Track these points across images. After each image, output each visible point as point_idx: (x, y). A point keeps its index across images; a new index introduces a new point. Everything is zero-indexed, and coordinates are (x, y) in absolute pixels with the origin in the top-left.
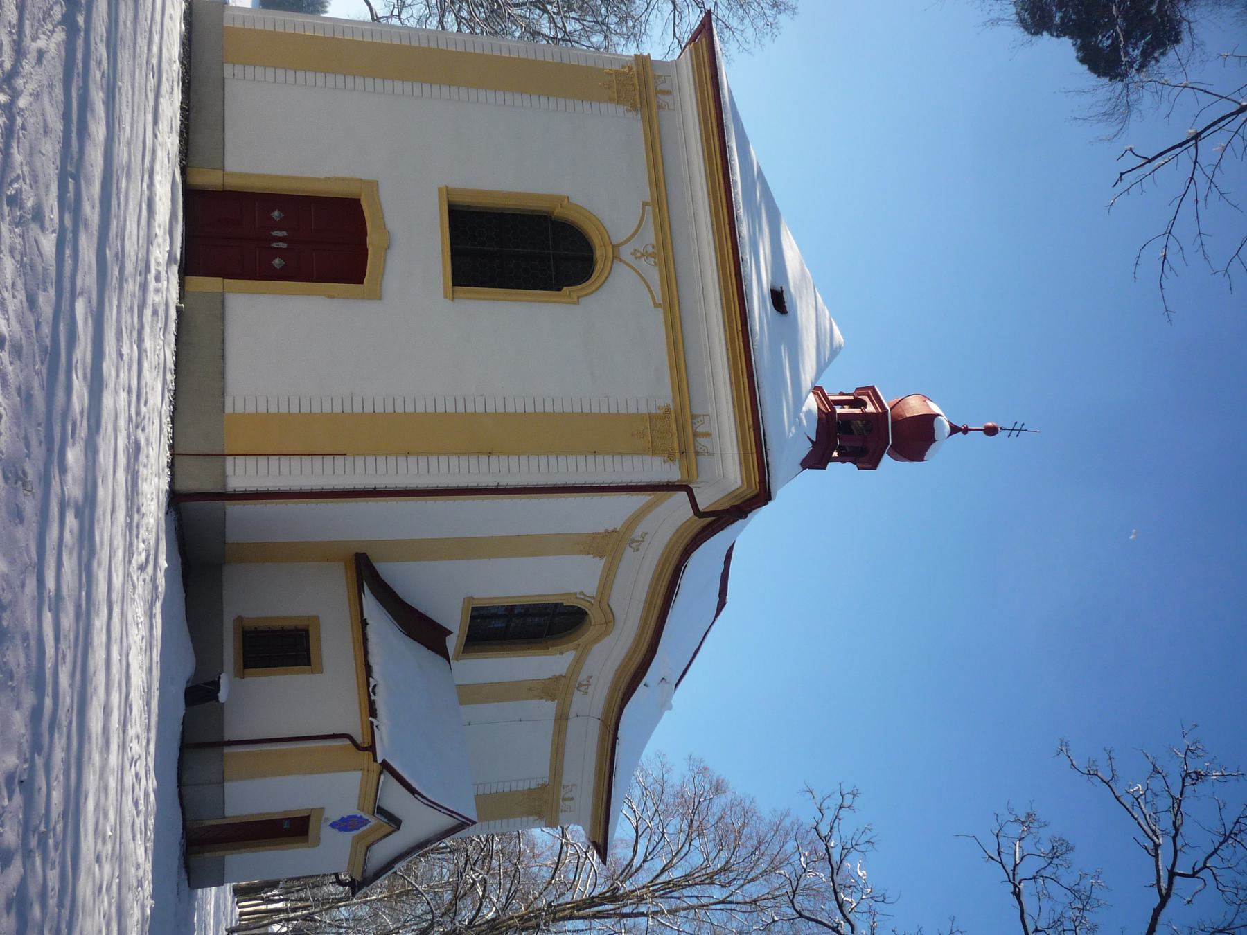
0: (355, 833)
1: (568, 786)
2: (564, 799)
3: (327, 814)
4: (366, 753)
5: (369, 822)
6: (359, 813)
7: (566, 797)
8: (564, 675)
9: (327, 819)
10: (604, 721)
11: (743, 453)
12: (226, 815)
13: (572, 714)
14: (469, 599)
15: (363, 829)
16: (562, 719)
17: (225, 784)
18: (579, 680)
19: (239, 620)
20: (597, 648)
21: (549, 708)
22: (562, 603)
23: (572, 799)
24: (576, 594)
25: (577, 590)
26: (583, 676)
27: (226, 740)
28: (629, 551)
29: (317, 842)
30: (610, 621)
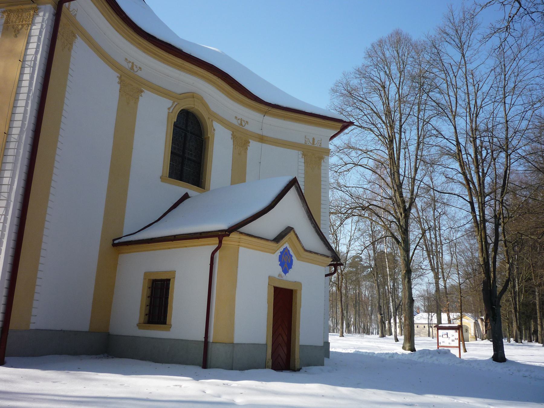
0: (294, 258)
1: (305, 141)
2: (313, 144)
3: (276, 276)
4: (223, 242)
5: (286, 247)
6: (278, 253)
7: (311, 142)
8: (232, 133)
9: (280, 275)
10: (265, 113)
12: (265, 343)
13: (260, 132)
15: (292, 253)
16: (262, 139)
17: (236, 341)
18: (237, 124)
19: (139, 326)
20: (213, 108)
21: (254, 146)
22: (175, 122)
23: (314, 139)
24: (169, 112)
25: (166, 111)
26: (235, 122)
27: (203, 340)
28: (139, 73)
29: (299, 284)
30: (193, 96)
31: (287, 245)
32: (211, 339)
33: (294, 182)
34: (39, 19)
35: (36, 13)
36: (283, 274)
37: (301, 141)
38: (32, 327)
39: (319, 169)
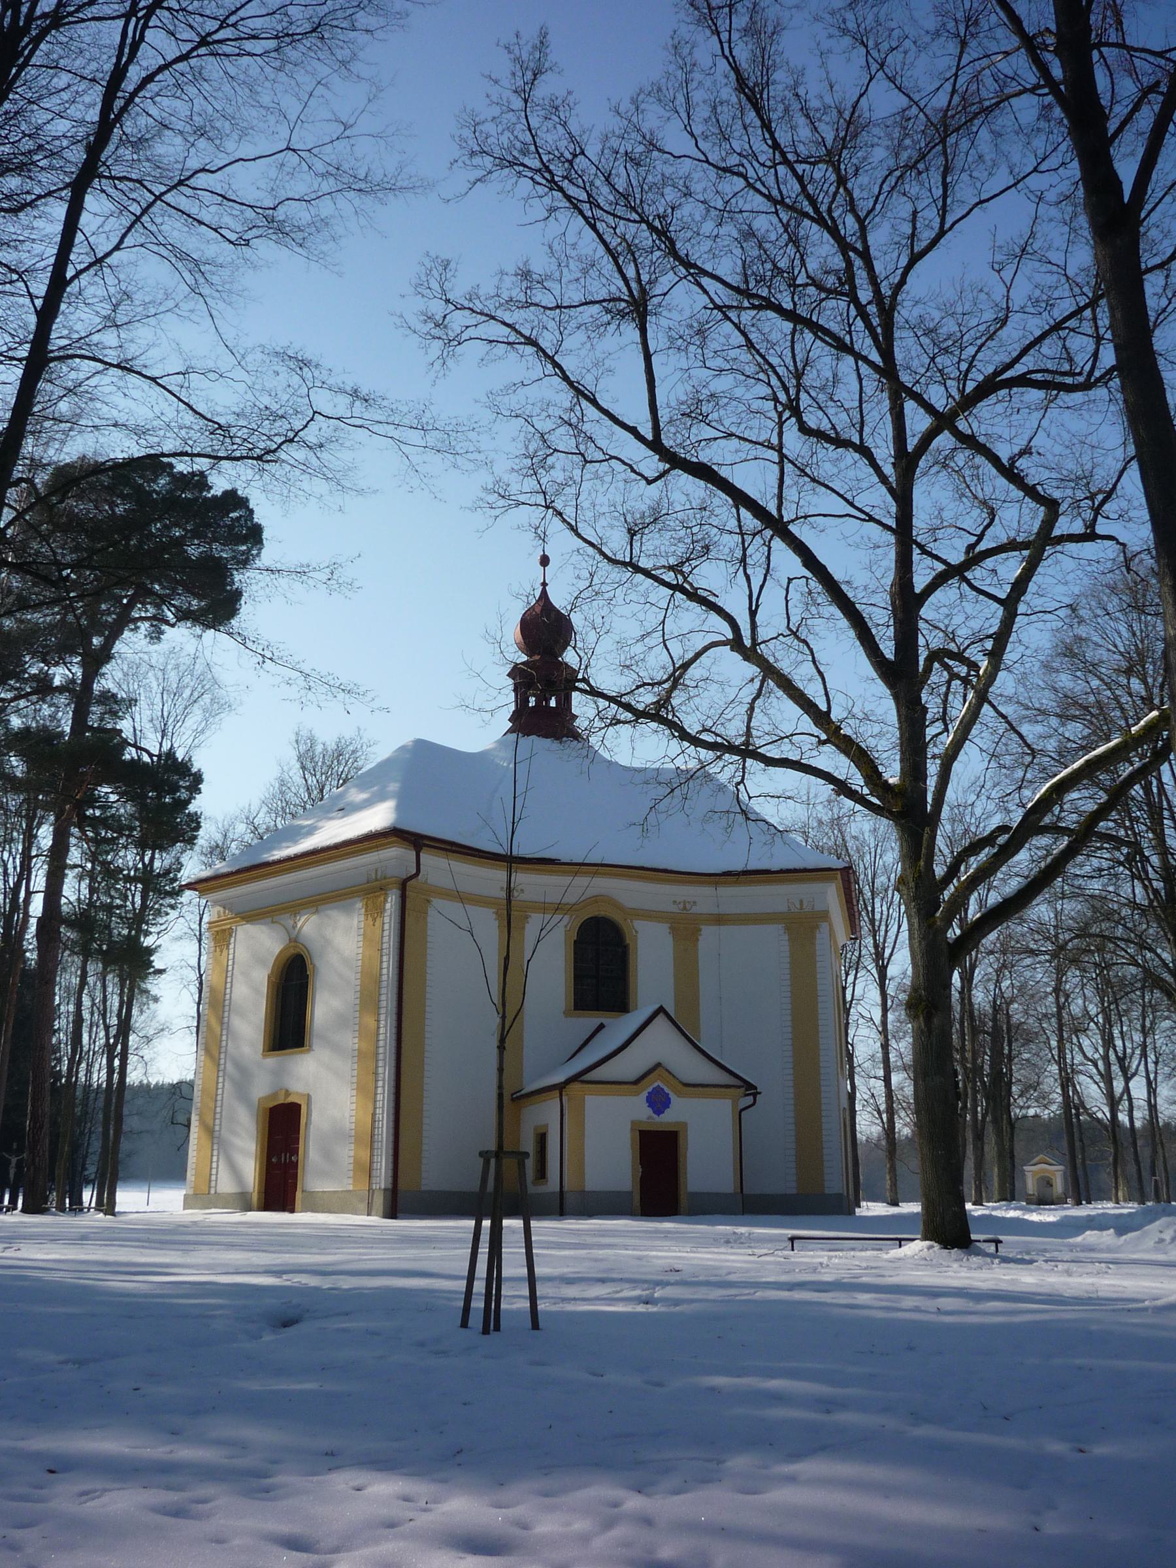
0: (672, 1096)
6: (645, 1094)
9: (649, 1118)
10: (716, 884)
11: (377, 848)
14: (567, 1013)
15: (667, 1090)
16: (720, 920)
17: (587, 1189)
21: (709, 936)
23: (801, 902)
29: (685, 1125)
30: (596, 899)
31: (659, 1083)
32: (566, 1189)
33: (661, 1010)
34: (388, 906)
35: (385, 901)
36: (655, 1116)
37: (782, 907)
38: (424, 1188)
39: (813, 944)
